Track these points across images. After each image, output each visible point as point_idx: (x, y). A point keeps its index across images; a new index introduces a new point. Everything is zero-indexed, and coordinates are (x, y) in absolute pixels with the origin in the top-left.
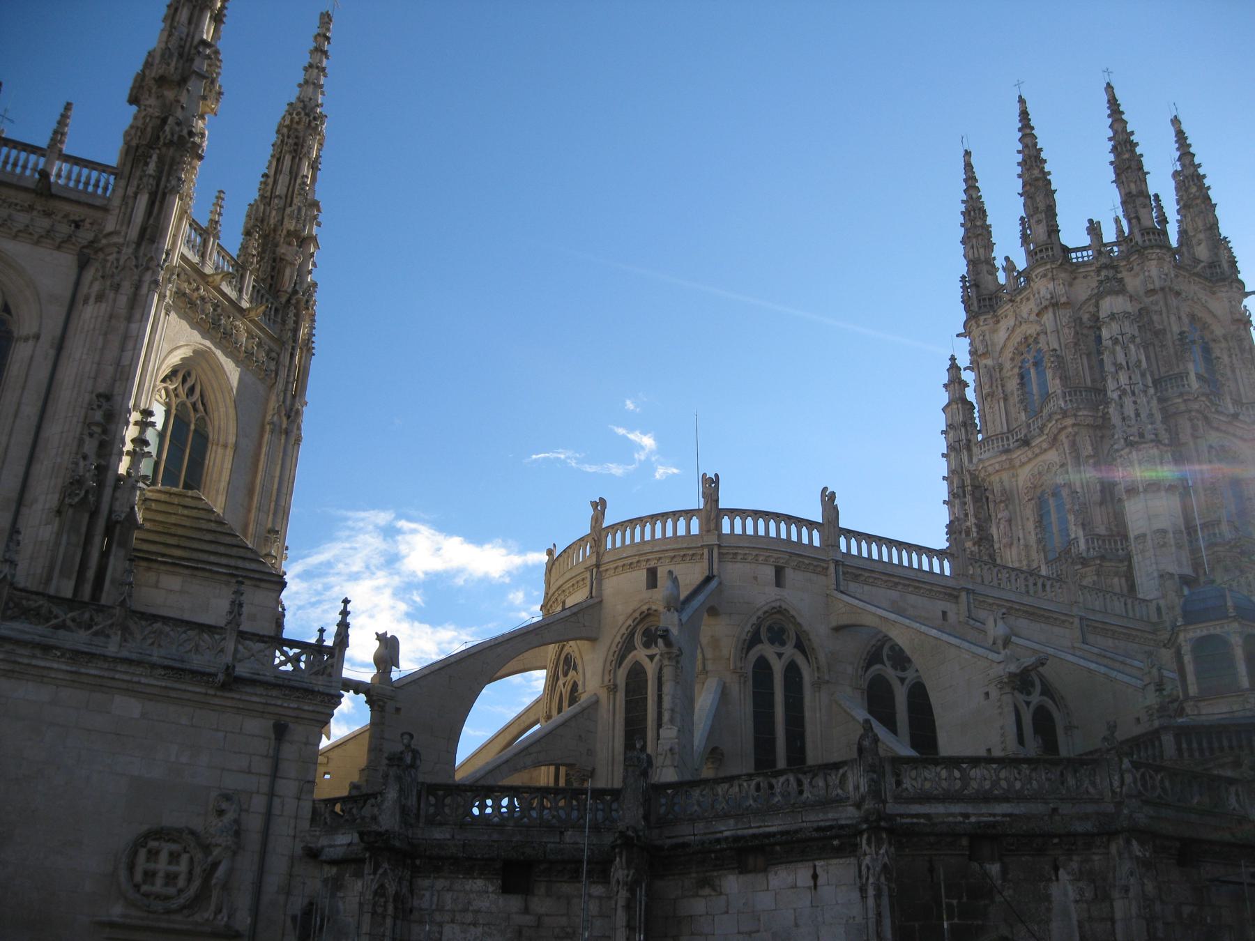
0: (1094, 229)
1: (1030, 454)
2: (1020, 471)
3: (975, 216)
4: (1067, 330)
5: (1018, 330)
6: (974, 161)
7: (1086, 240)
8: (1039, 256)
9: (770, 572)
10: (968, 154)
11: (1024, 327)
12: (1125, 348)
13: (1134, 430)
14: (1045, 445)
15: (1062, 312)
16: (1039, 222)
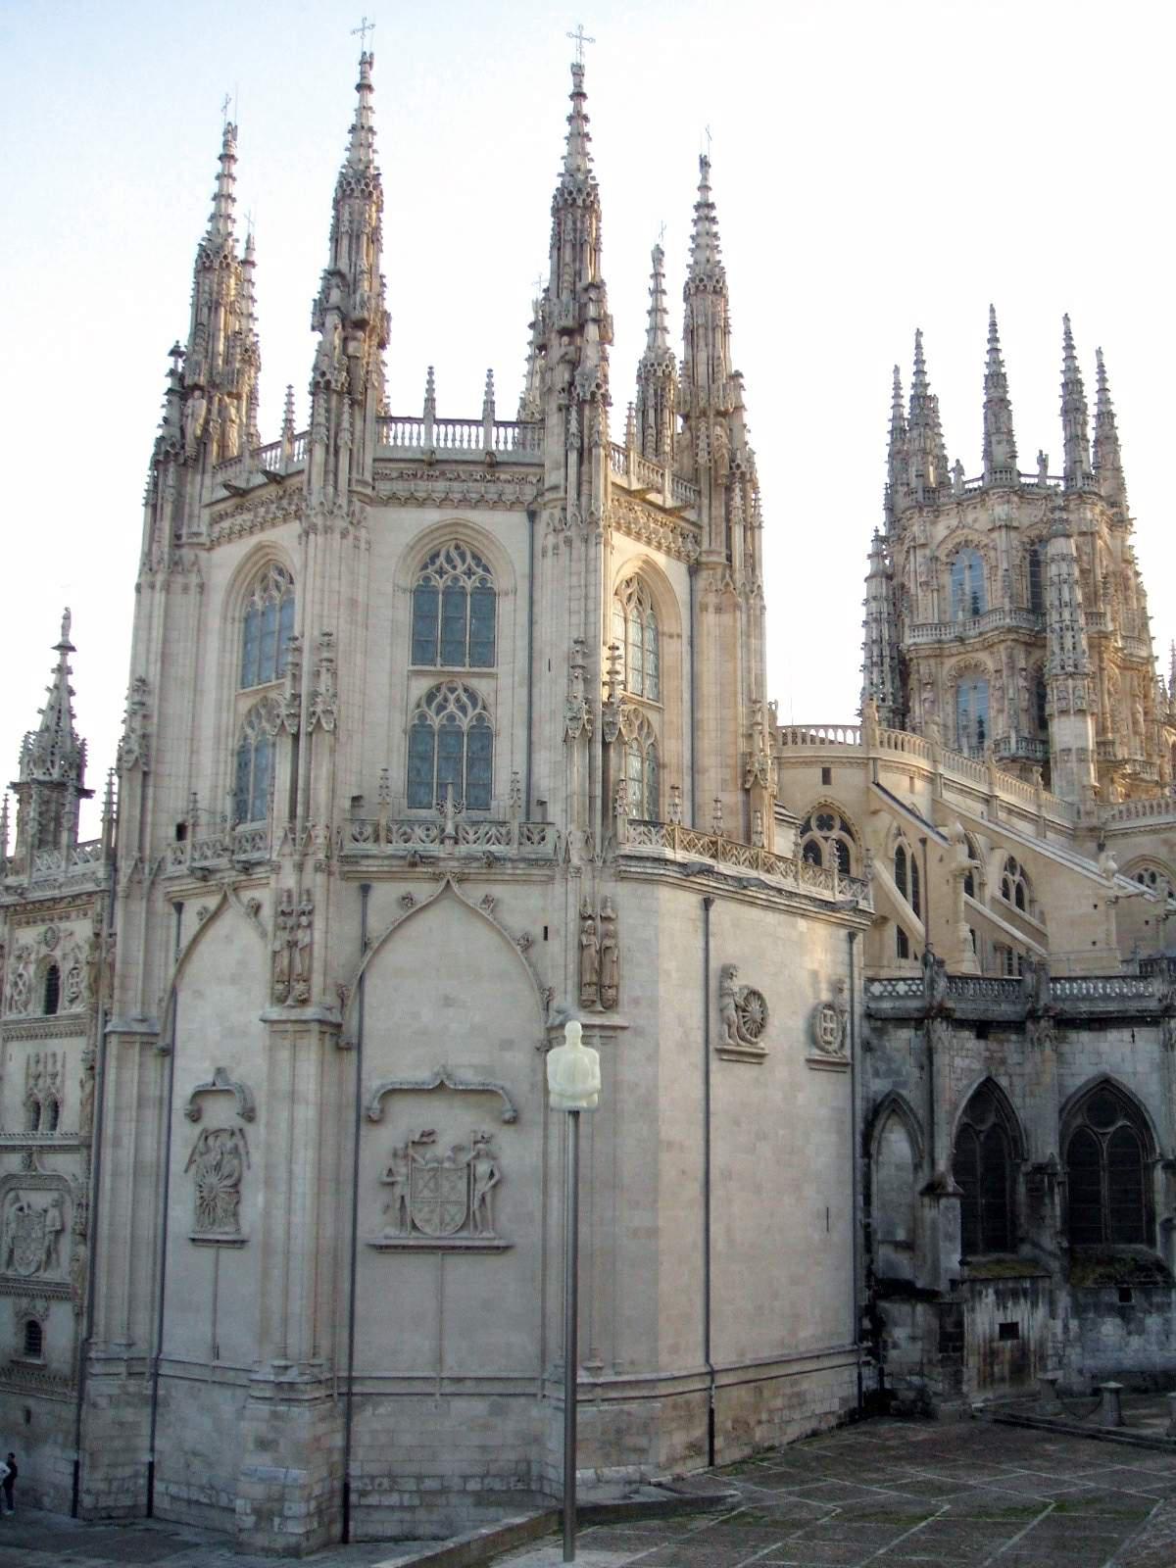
0: (1043, 461)
1: (962, 649)
2: (946, 660)
3: (897, 386)
4: (1014, 552)
5: (959, 532)
6: (923, 341)
7: (1035, 469)
8: (998, 476)
9: (907, 780)
10: (919, 334)
11: (966, 531)
12: (1071, 589)
13: (1071, 662)
14: (977, 646)
15: (1013, 534)
16: (999, 443)
